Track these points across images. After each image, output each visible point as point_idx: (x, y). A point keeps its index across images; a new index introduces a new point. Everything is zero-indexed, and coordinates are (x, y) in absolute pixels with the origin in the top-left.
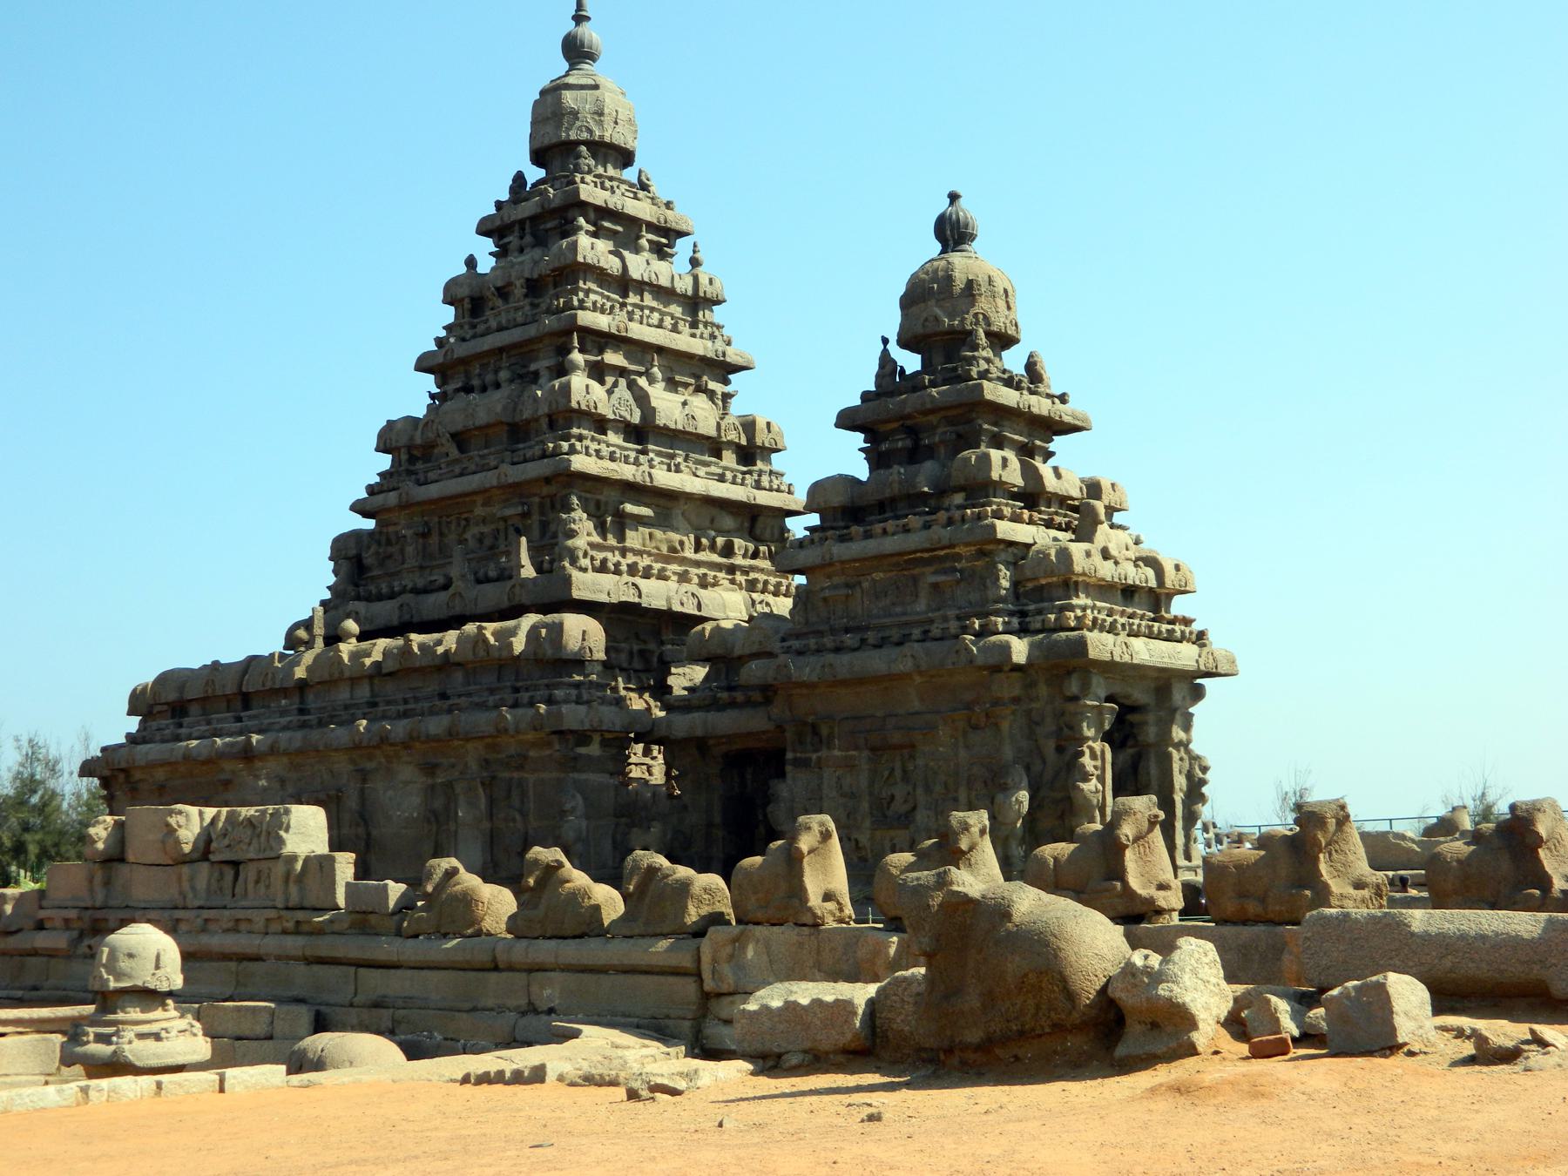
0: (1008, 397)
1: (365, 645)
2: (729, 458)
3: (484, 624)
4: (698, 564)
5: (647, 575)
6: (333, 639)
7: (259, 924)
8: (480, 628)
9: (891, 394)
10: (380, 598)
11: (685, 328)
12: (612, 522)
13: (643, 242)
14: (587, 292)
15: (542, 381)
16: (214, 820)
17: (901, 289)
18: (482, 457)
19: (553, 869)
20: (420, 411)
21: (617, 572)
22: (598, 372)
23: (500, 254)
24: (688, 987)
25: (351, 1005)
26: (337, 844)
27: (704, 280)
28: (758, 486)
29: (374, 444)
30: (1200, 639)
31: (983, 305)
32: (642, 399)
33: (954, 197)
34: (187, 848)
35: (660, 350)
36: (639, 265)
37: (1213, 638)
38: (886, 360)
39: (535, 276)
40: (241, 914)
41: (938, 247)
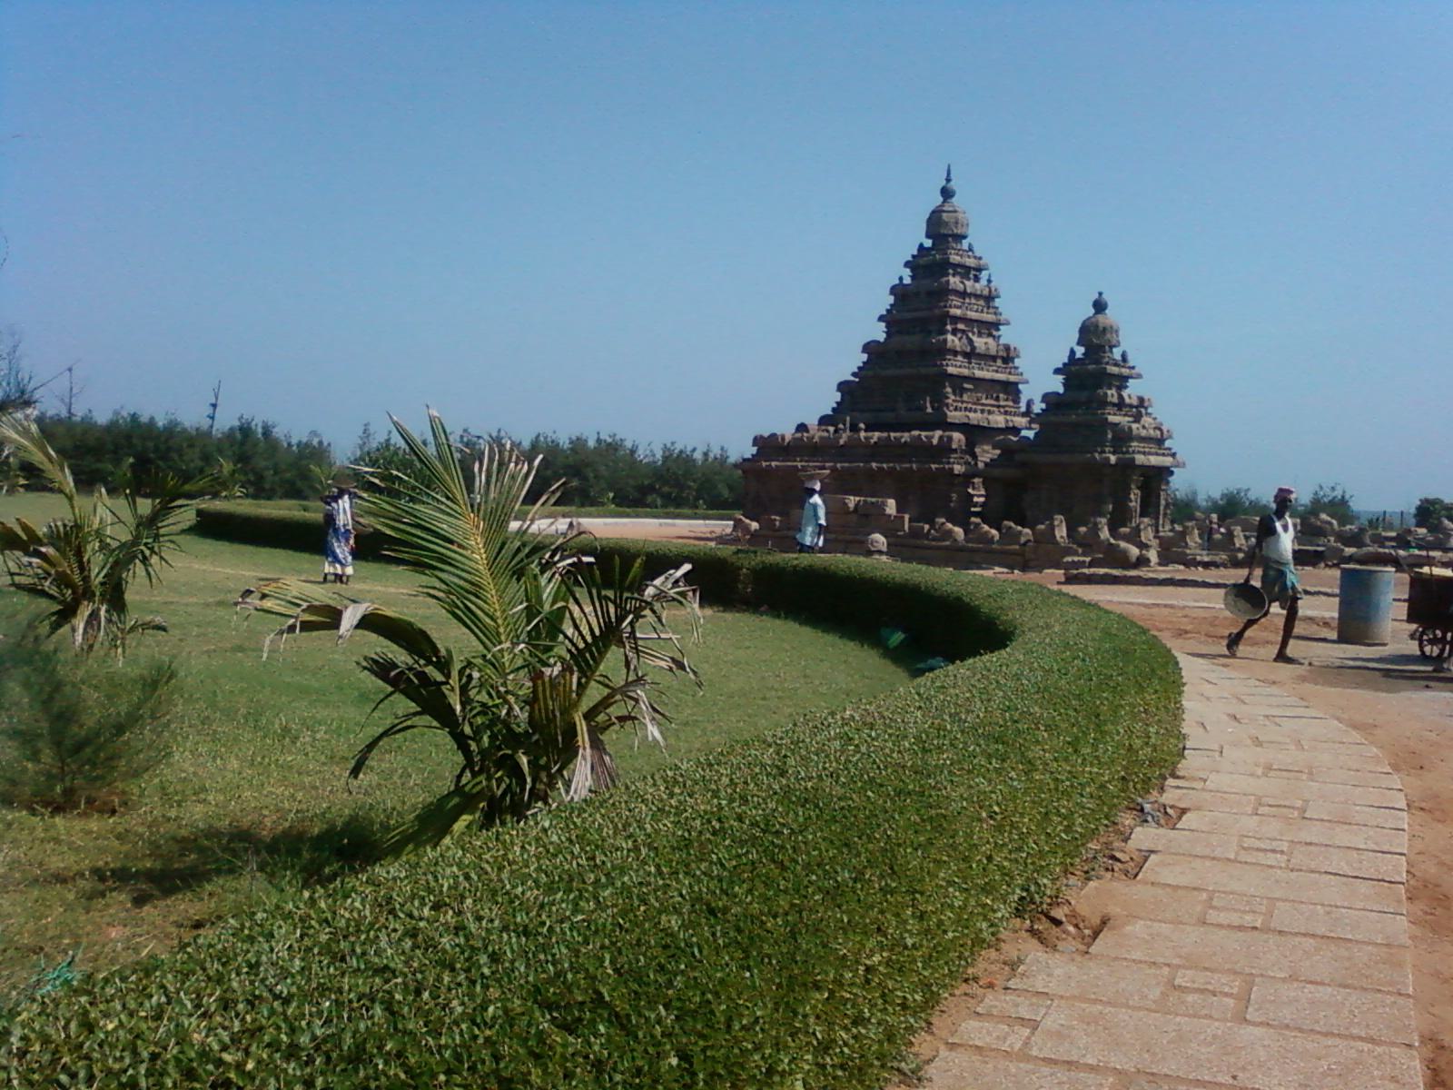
0: (1115, 370)
1: (870, 434)
2: (999, 362)
5: (970, 410)
6: (854, 428)
9: (1073, 365)
11: (985, 310)
12: (959, 391)
13: (971, 276)
17: (1079, 325)
19: (977, 525)
20: (882, 340)
22: (954, 332)
23: (913, 278)
28: (1010, 373)
30: (1174, 455)
31: (1108, 336)
32: (971, 342)
33: (1100, 294)
34: (851, 509)
35: (976, 321)
36: (970, 285)
37: (1178, 456)
38: (1072, 352)
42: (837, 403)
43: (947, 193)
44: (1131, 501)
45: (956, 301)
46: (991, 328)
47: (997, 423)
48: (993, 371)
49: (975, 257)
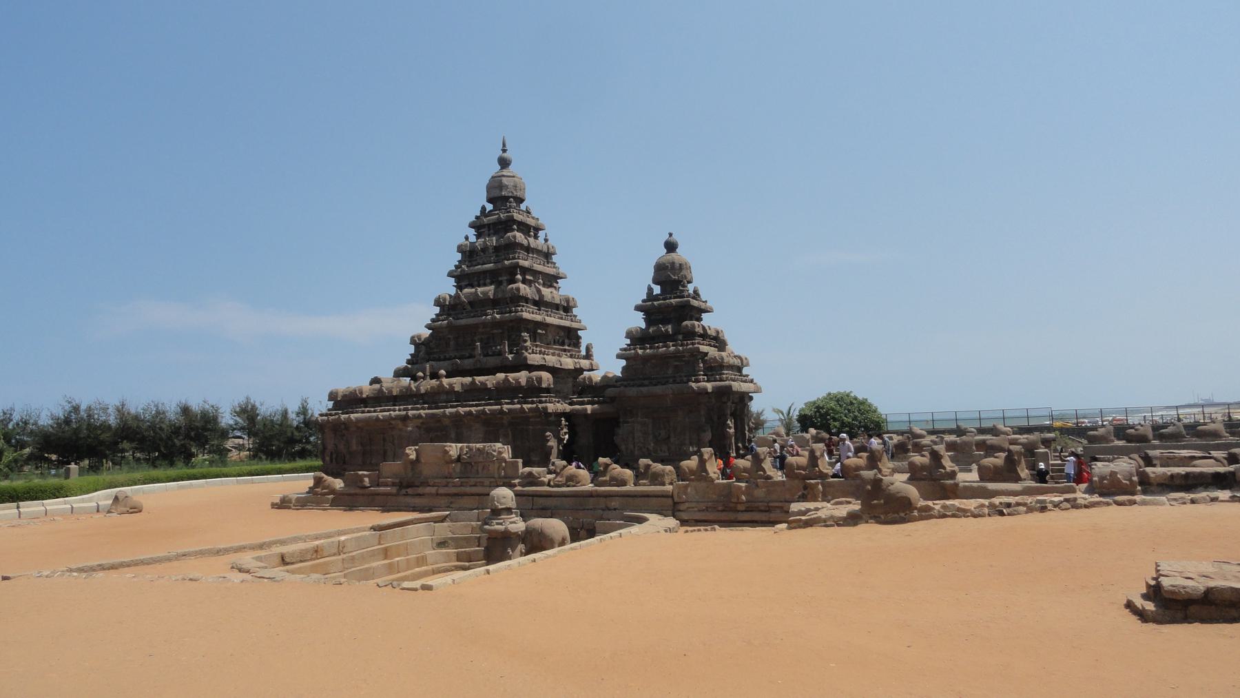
3: (508, 374)
4: (556, 349)
7: (488, 483)
8: (506, 376)
10: (439, 360)
14: (519, 253)
15: (505, 284)
16: (461, 449)
18: (482, 311)
19: (607, 466)
21: (536, 353)
23: (478, 236)
24: (670, 501)
25: (532, 509)
26: (515, 455)
27: (551, 247)
28: (572, 321)
29: (433, 304)
30: (752, 381)
32: (539, 291)
33: (671, 235)
35: (540, 273)
38: (650, 289)
39: (497, 245)
40: (479, 480)
41: (665, 251)
42: (411, 355)
43: (504, 163)
44: (730, 428)
45: (523, 253)
46: (552, 280)
47: (567, 364)
48: (559, 318)
49: (533, 218)
